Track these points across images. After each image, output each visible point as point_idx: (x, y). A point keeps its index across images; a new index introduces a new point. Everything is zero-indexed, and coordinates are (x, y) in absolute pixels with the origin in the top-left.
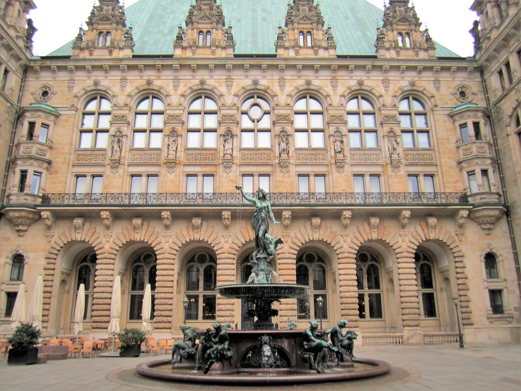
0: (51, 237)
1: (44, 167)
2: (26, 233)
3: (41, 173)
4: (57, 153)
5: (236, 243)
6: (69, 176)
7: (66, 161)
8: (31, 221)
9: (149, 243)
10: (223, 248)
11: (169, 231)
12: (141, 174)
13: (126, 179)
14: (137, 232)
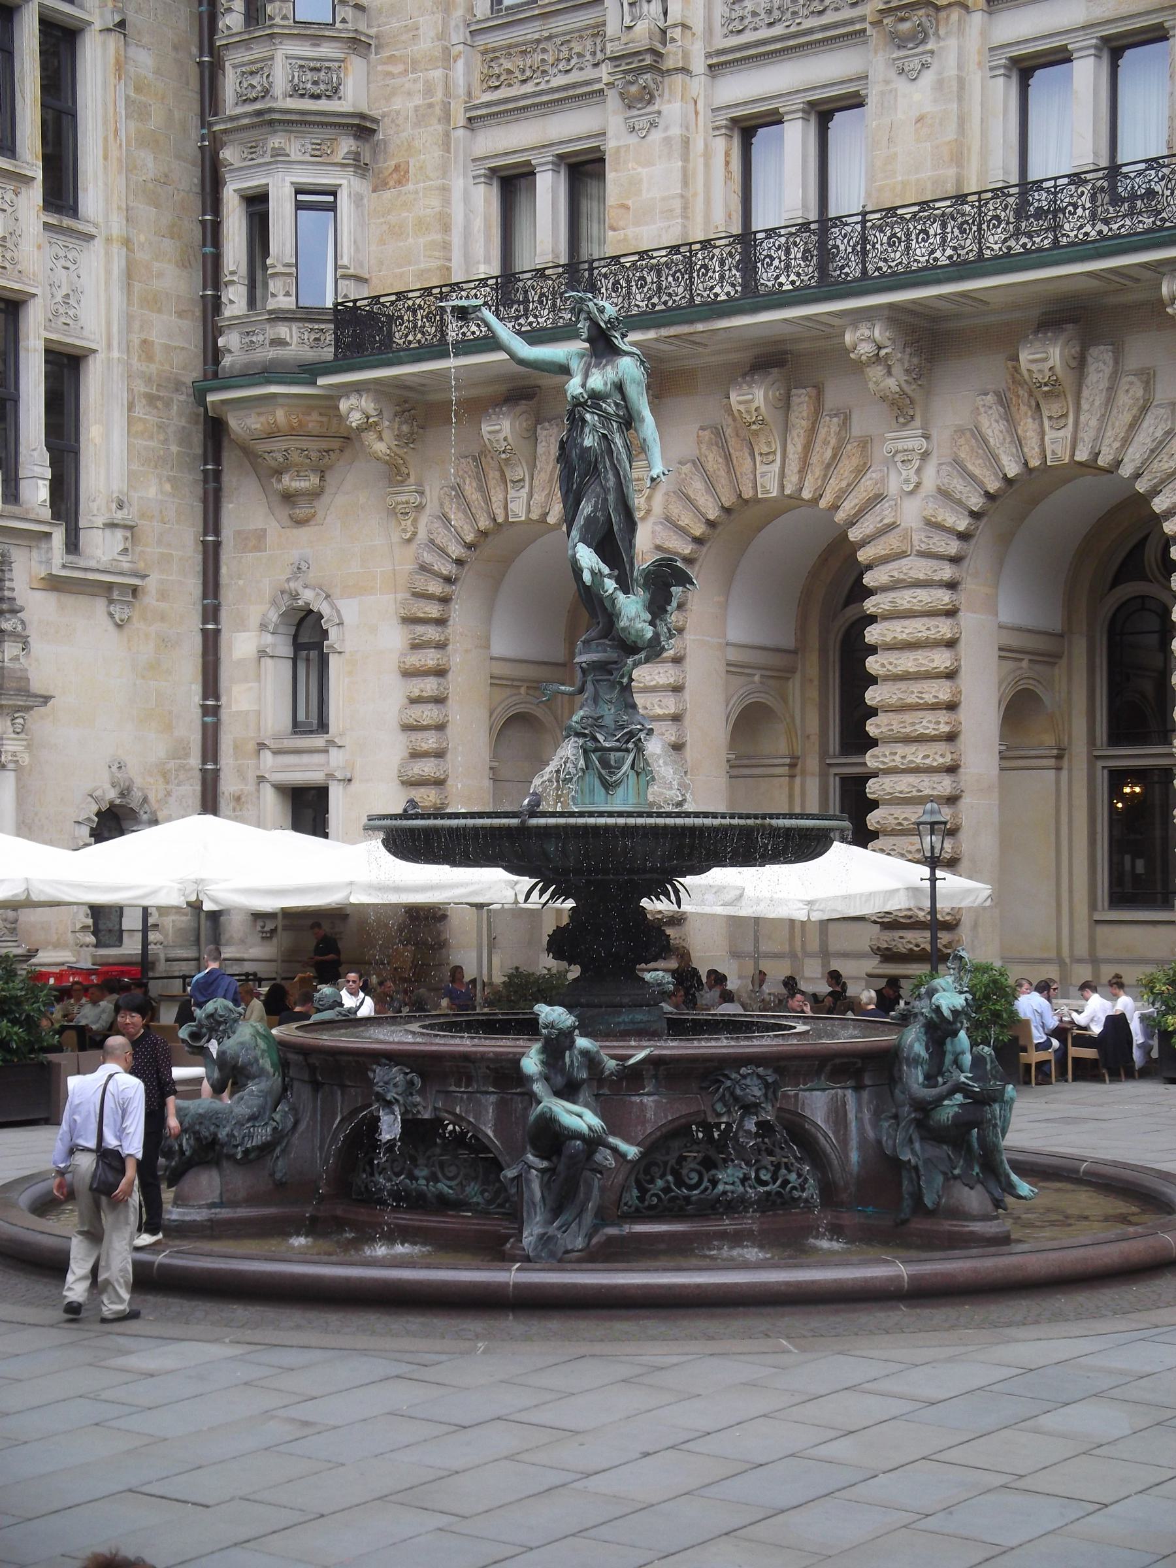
0: (412, 515)
1: (338, 160)
2: (320, 504)
3: (334, 194)
4: (390, 68)
6: (458, 184)
7: (431, 106)
8: (324, 444)
9: (823, 504)
12: (775, 112)
13: (707, 155)
14: (765, 450)
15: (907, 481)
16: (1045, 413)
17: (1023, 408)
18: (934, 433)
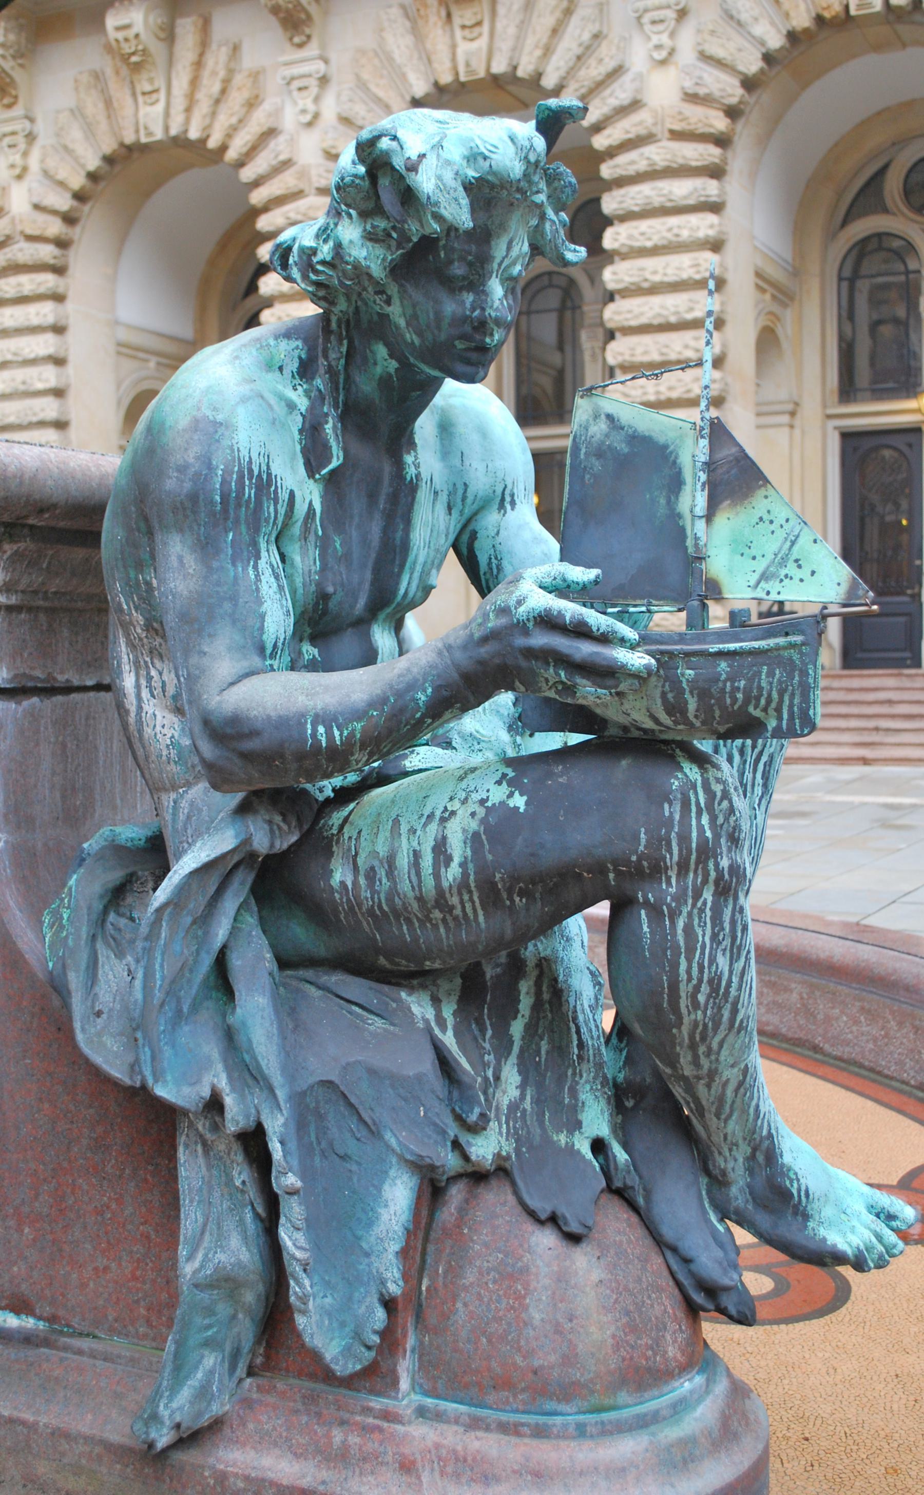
5: (720, 53)
10: (635, 105)
11: (312, 50)
14: (148, 88)
15: (304, 111)
16: (457, 21)
17: (433, 19)
18: (333, 56)
